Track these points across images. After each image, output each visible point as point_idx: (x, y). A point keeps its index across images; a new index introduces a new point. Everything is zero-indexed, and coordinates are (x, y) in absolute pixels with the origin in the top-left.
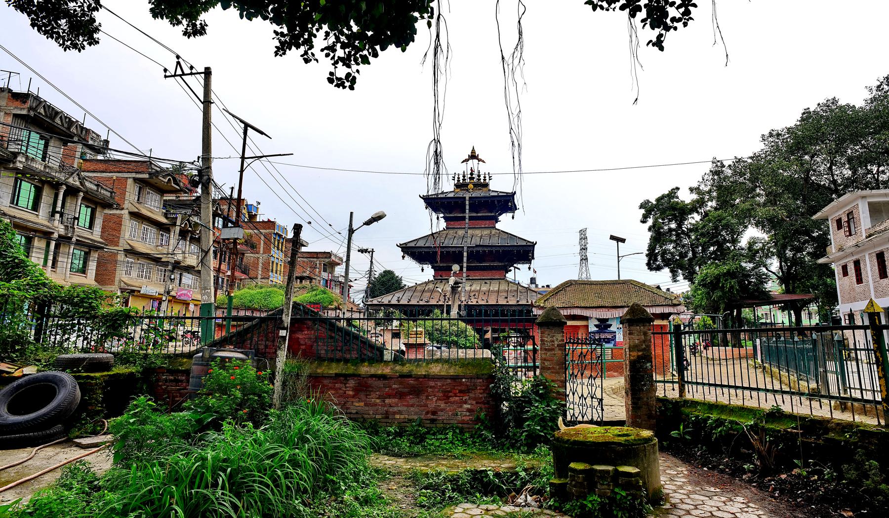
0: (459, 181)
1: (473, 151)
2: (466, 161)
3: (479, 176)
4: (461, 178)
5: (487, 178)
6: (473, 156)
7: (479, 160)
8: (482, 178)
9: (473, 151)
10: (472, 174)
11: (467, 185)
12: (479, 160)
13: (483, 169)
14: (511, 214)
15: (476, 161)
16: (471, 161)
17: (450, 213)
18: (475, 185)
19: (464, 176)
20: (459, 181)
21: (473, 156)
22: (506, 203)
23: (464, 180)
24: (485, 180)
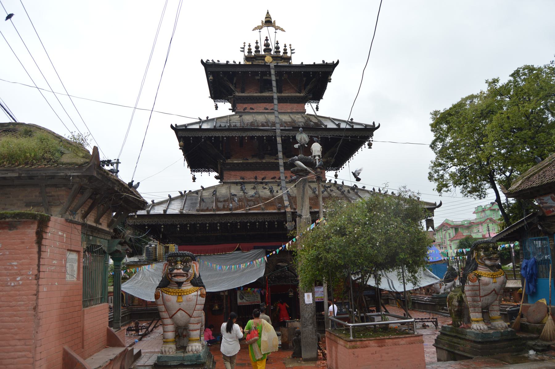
0: (250, 51)
1: (268, 16)
2: (259, 28)
3: (277, 48)
4: (253, 50)
5: (289, 51)
6: (268, 22)
7: (277, 28)
8: (282, 50)
9: (268, 16)
10: (267, 45)
11: (264, 56)
12: (277, 28)
13: (281, 39)
14: (314, 105)
15: (272, 29)
16: (265, 29)
17: (243, 92)
18: (275, 58)
19: (257, 47)
20: (250, 51)
21: (268, 22)
22: (316, 79)
23: (257, 51)
24: (285, 52)
